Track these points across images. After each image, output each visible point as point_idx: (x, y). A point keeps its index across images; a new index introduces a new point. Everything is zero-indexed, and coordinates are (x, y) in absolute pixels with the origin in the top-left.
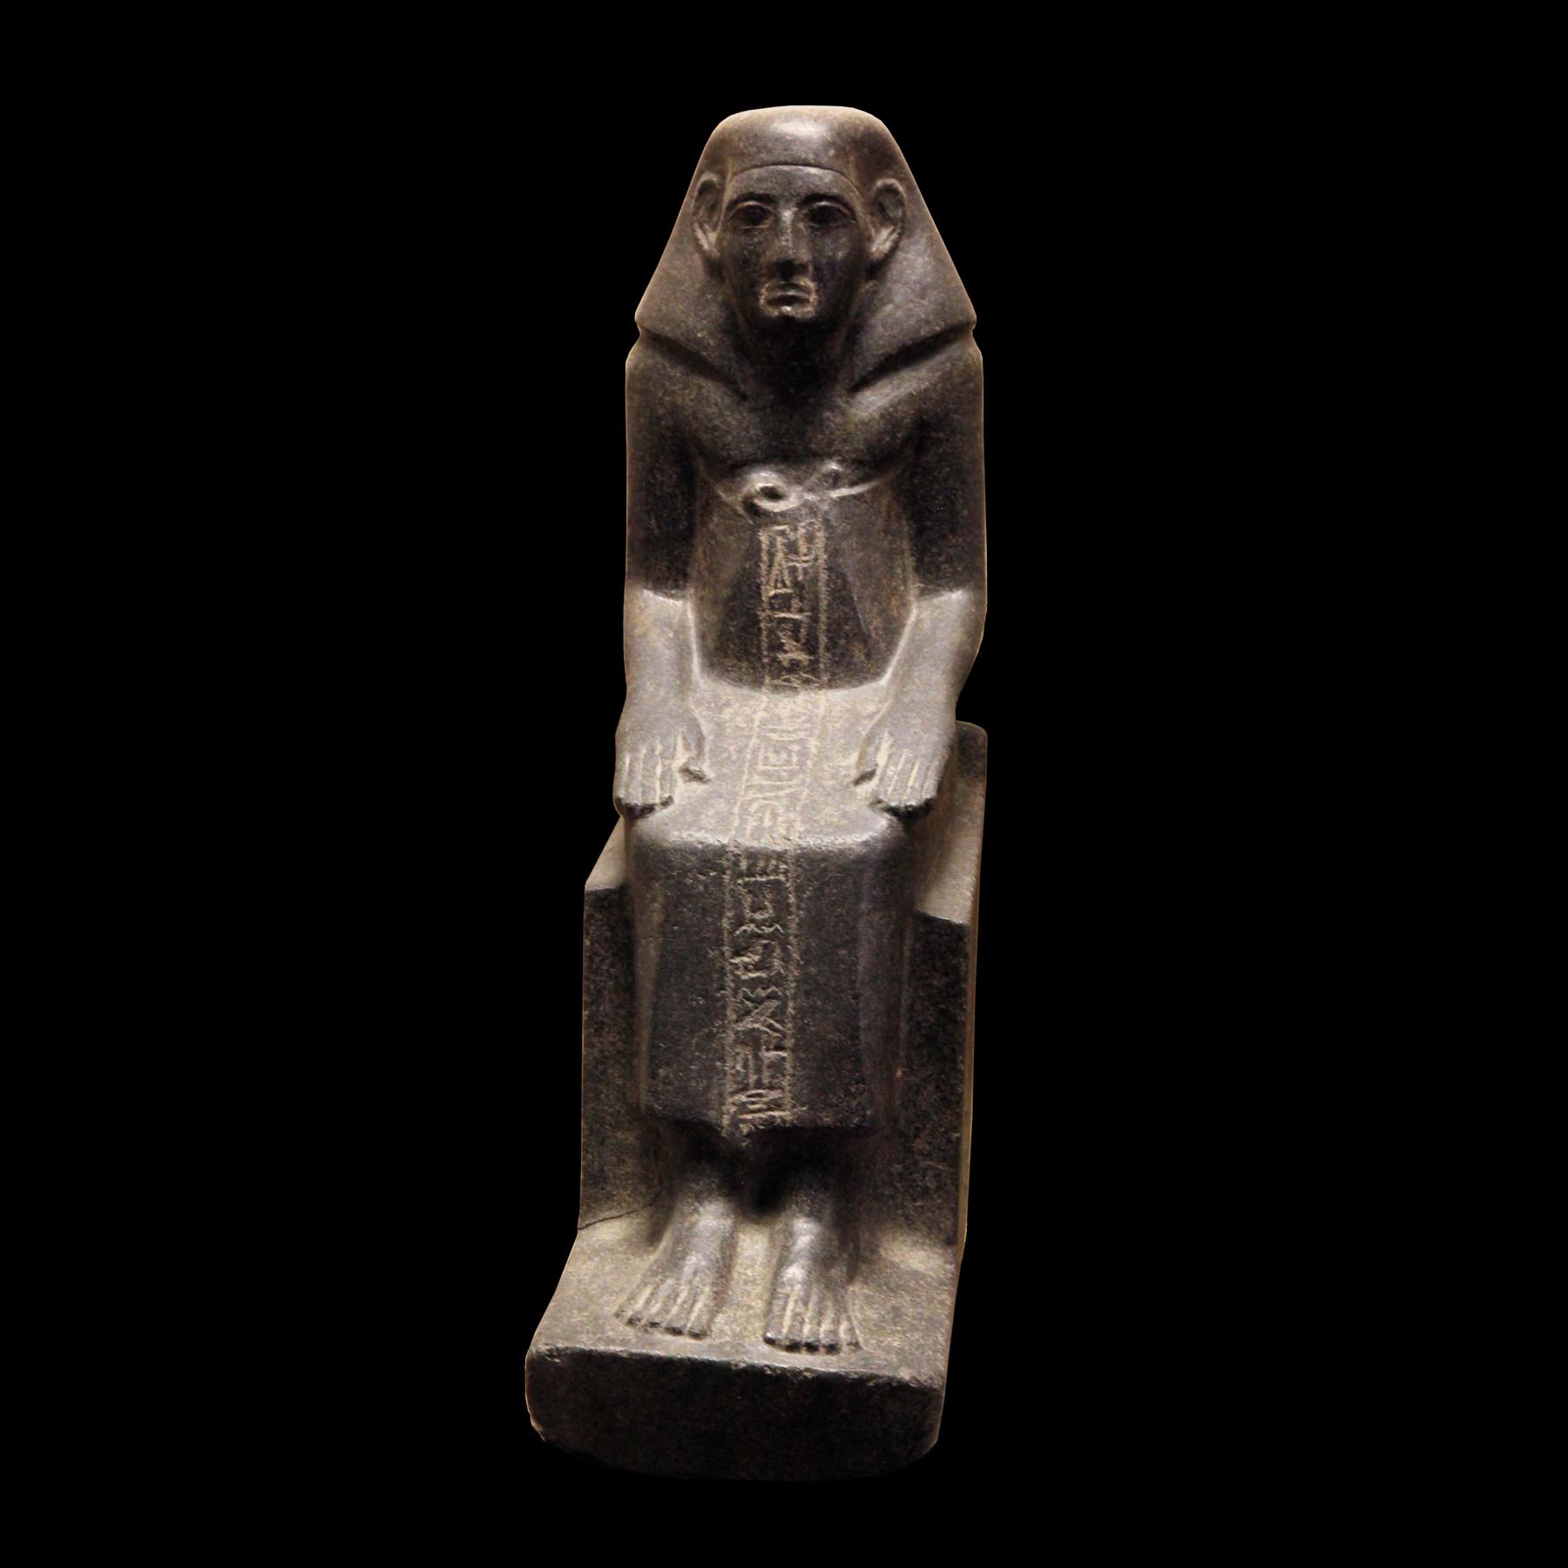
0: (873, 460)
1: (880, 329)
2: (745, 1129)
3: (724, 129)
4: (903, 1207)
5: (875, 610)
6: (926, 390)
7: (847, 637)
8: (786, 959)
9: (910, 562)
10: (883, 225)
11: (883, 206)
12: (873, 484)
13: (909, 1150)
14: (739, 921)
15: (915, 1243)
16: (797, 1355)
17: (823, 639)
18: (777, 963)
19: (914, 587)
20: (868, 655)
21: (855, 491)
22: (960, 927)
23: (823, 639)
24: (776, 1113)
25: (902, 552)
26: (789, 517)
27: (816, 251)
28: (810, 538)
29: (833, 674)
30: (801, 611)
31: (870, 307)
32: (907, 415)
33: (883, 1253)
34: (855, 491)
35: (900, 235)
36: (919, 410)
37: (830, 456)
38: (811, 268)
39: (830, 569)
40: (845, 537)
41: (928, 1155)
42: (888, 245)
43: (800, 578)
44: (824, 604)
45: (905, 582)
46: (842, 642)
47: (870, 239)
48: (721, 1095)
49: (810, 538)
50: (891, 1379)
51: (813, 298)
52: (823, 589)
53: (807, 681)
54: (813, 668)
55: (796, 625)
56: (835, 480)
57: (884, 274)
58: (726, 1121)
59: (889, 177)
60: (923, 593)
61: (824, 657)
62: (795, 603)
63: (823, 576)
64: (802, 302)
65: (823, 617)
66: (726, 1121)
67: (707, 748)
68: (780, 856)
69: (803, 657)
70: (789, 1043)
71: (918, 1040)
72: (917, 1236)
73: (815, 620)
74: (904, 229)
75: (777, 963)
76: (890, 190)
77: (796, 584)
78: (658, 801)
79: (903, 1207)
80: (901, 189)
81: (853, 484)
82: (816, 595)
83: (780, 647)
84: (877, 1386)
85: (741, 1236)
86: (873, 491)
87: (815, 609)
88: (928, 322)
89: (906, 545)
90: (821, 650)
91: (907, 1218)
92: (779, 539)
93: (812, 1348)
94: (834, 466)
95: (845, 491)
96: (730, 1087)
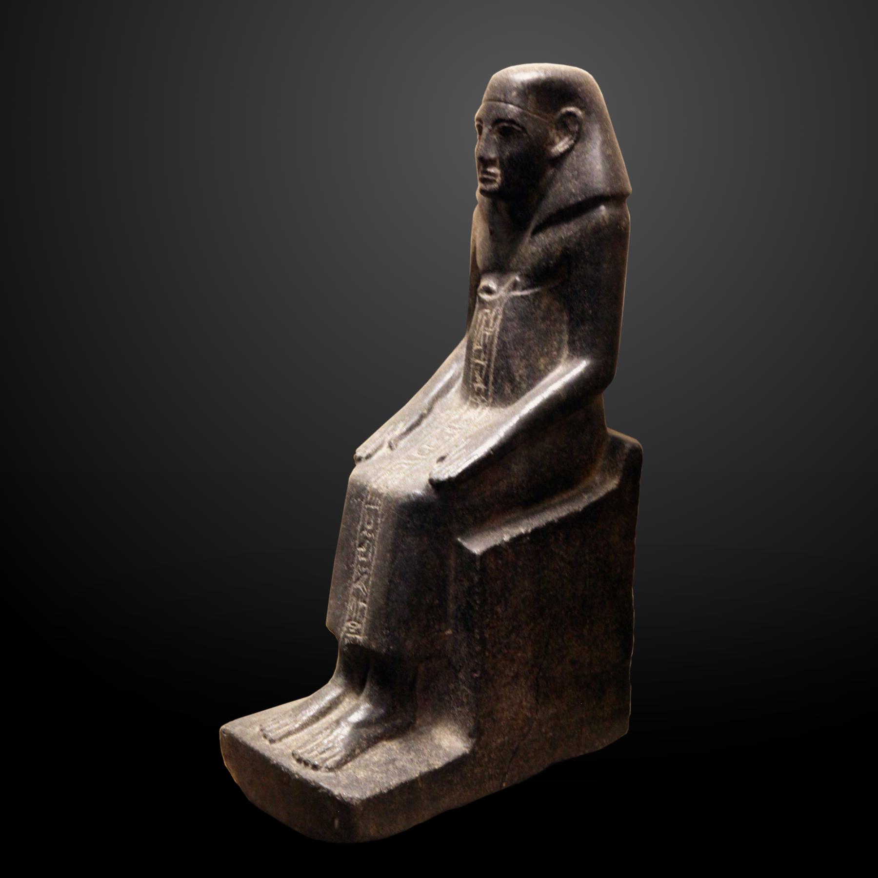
0: (537, 277)
1: (551, 199)
2: (346, 641)
3: (496, 79)
4: (453, 708)
5: (522, 364)
6: (570, 236)
7: (502, 378)
8: (373, 553)
9: (566, 338)
10: (565, 135)
11: (565, 124)
12: (536, 290)
13: (457, 677)
14: (363, 529)
15: (454, 731)
16: (298, 765)
17: (491, 378)
18: (370, 555)
19: (565, 353)
20: (512, 391)
21: (525, 293)
22: (474, 555)
23: (491, 378)
24: (358, 637)
25: (560, 332)
26: (492, 304)
27: (500, 151)
28: (495, 319)
29: (494, 399)
30: (484, 360)
31: (550, 183)
32: (557, 249)
33: (433, 731)
34: (525, 293)
35: (576, 142)
36: (566, 249)
37: (516, 271)
38: (498, 162)
39: (499, 338)
40: (511, 320)
41: (464, 683)
42: (567, 147)
43: (487, 341)
44: (493, 359)
45: (559, 350)
46: (499, 381)
47: (553, 144)
48: (343, 621)
49: (495, 319)
50: (329, 791)
51: (498, 179)
52: (495, 349)
53: (483, 401)
54: (486, 395)
55: (482, 367)
56: (515, 286)
57: (561, 165)
58: (342, 635)
59: (570, 106)
60: (570, 358)
61: (491, 388)
62: (483, 356)
63: (496, 341)
64: (492, 182)
65: (492, 365)
66: (342, 635)
67: (417, 429)
68: (379, 495)
69: (482, 387)
70: (368, 600)
71: (459, 615)
72: (456, 727)
73: (489, 366)
74: (579, 137)
75: (370, 555)
76: (570, 114)
77: (485, 346)
78: (364, 455)
79: (453, 708)
80: (580, 113)
81: (524, 289)
82: (491, 351)
83: (474, 380)
84: (322, 792)
85: (347, 699)
86: (536, 295)
87: (489, 360)
88: (574, 195)
89: (564, 327)
90: (490, 384)
91: (454, 715)
92: (485, 318)
93: (306, 763)
94: (518, 279)
95: (518, 293)
96: (347, 618)
